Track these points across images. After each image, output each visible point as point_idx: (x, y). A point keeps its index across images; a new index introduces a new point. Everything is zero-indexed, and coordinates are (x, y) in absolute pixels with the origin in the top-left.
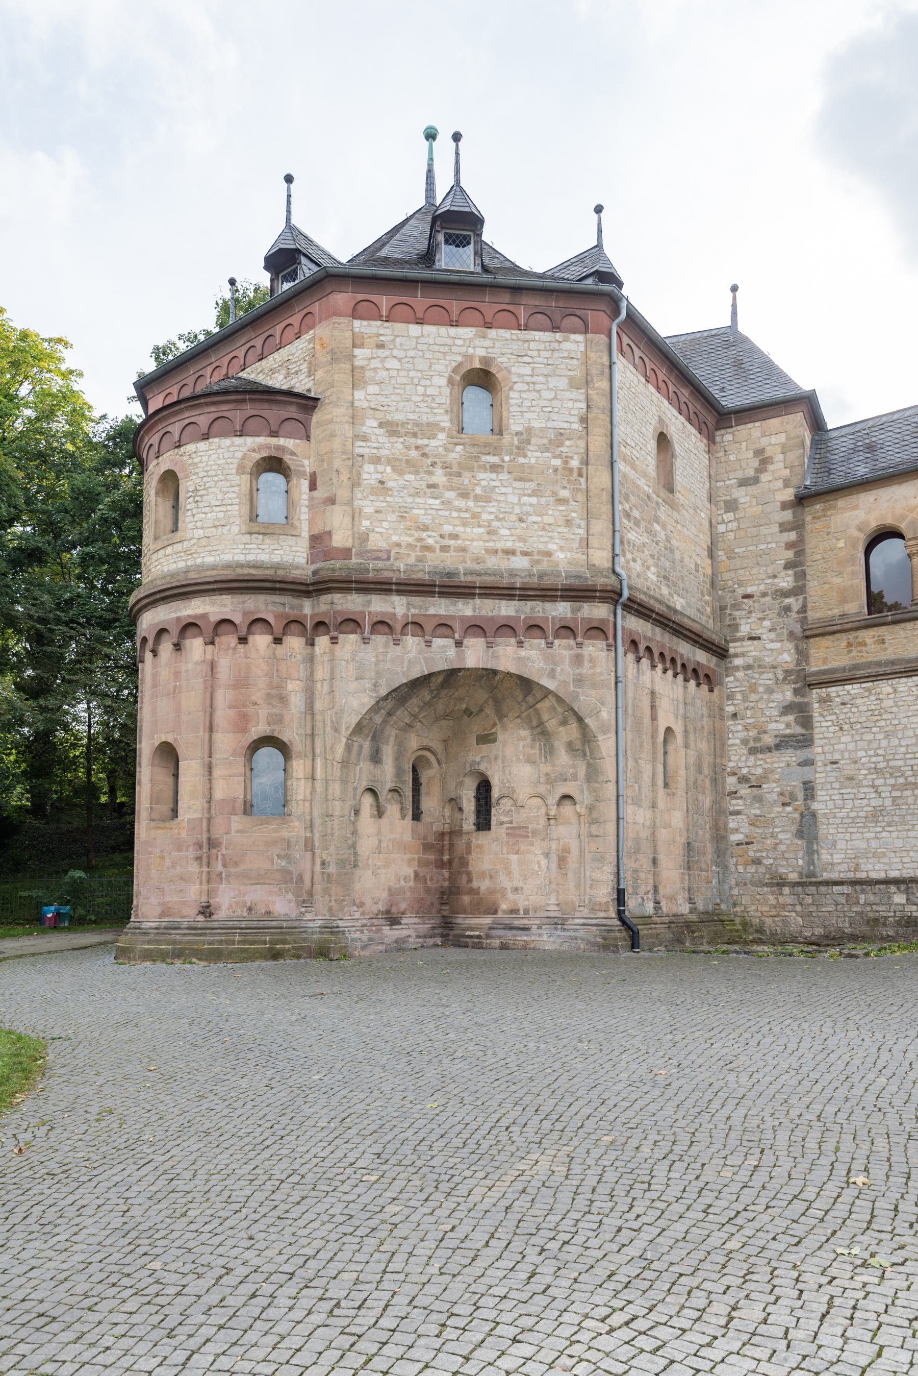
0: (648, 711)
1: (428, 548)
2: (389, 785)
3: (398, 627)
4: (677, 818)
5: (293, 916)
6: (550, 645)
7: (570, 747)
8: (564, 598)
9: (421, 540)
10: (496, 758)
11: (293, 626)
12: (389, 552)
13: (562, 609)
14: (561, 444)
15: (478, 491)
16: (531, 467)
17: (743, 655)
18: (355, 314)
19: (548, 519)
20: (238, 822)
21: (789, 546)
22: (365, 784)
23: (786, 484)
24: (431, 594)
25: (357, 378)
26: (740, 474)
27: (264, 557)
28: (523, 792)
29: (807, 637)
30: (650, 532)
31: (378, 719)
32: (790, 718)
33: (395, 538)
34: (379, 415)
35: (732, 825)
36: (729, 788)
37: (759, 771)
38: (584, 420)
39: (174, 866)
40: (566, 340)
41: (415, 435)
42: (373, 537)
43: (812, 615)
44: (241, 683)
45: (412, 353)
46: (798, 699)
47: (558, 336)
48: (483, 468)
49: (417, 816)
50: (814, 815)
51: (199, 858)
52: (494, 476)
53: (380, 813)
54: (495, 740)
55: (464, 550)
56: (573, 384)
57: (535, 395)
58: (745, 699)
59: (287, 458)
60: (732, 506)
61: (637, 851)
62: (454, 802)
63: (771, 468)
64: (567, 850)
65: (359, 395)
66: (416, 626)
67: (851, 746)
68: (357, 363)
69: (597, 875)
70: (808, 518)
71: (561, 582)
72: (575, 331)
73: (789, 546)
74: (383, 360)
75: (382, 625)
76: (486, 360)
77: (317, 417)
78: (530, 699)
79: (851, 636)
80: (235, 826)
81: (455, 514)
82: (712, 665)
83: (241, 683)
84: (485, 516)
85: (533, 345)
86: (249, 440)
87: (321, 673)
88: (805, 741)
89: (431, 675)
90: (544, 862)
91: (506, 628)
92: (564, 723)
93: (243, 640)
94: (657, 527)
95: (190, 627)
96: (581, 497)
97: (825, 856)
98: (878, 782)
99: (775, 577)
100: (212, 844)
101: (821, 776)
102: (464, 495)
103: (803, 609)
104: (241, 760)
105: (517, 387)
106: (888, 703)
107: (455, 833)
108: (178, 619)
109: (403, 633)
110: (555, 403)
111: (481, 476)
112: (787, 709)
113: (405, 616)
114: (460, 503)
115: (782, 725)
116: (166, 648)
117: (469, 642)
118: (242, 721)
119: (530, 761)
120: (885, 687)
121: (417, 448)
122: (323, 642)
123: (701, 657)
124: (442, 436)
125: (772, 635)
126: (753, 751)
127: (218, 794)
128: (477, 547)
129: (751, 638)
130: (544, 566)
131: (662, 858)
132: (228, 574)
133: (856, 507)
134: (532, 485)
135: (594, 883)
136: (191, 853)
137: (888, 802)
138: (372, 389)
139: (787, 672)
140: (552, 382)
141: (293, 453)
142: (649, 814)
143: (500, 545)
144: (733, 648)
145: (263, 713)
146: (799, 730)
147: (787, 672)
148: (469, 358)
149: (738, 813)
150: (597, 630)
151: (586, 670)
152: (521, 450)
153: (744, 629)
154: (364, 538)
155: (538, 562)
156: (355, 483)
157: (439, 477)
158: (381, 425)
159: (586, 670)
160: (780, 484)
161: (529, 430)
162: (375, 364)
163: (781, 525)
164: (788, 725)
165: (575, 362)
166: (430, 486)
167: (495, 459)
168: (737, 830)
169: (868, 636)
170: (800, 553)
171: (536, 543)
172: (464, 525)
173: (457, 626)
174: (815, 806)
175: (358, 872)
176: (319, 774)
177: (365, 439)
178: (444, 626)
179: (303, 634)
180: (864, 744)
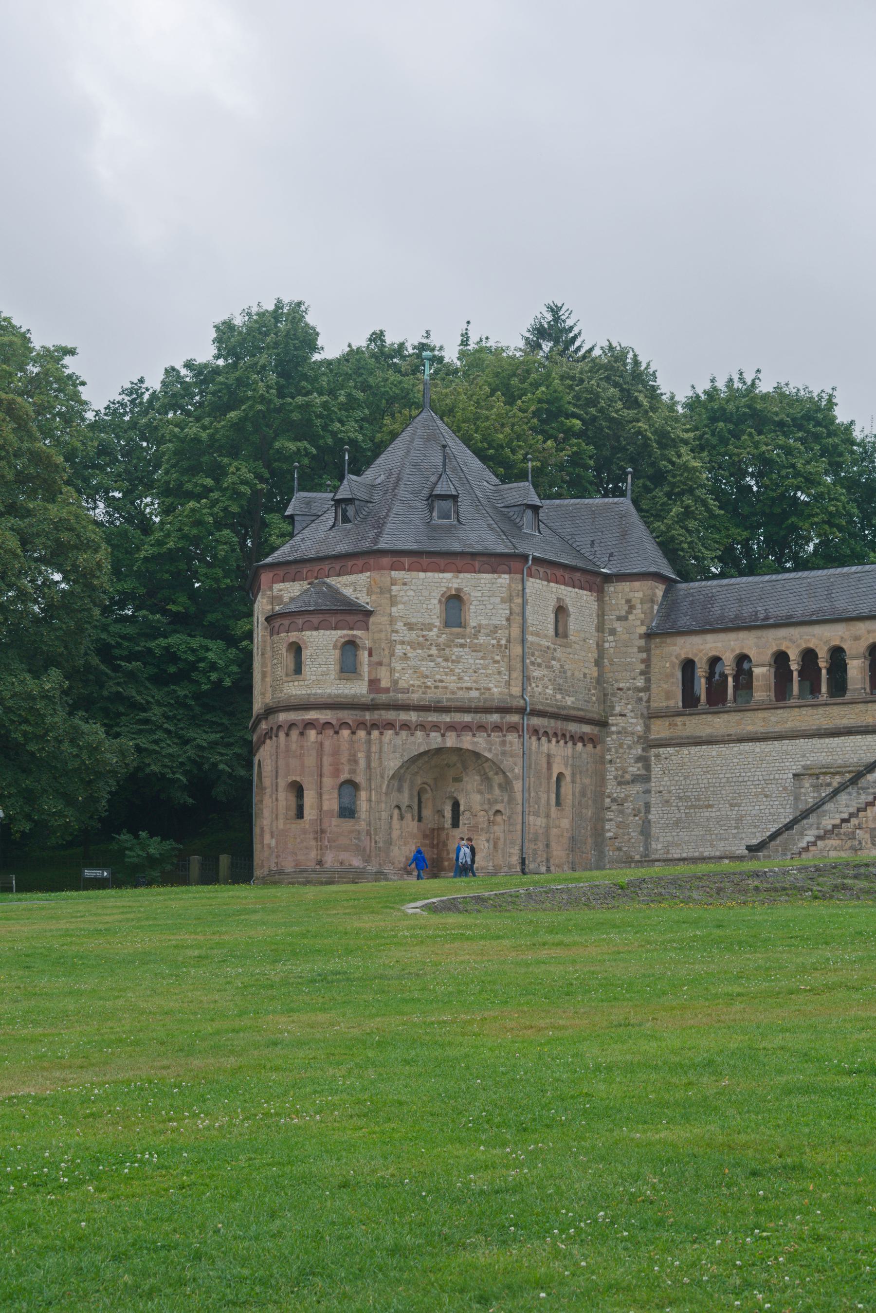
0: (545, 766)
1: (428, 687)
2: (406, 804)
3: (413, 727)
4: (565, 823)
5: (361, 867)
6: (489, 736)
7: (500, 785)
8: (496, 712)
9: (424, 683)
10: (462, 790)
11: (361, 726)
12: (408, 689)
13: (495, 718)
14: (497, 632)
15: (454, 657)
17: (616, 725)
18: (393, 568)
20: (335, 821)
21: (643, 661)
22: (395, 803)
23: (642, 624)
24: (429, 711)
25: (393, 601)
26: (617, 613)
27: (346, 691)
28: (477, 807)
29: (650, 718)
30: (549, 667)
31: (402, 771)
32: (640, 765)
33: (411, 682)
34: (404, 620)
35: (607, 827)
36: (606, 805)
37: (623, 795)
38: (508, 619)
39: (302, 842)
40: (500, 577)
41: (422, 630)
42: (400, 682)
43: (654, 705)
44: (336, 753)
45: (420, 587)
46: (644, 754)
47: (495, 576)
48: (456, 646)
49: (420, 819)
50: (649, 822)
51: (316, 839)
52: (461, 650)
53: (402, 818)
54: (462, 781)
55: (446, 688)
56: (503, 601)
58: (617, 752)
59: (358, 641)
60: (613, 632)
61: (536, 840)
62: (440, 813)
63: (634, 612)
64: (498, 839)
65: (394, 609)
66: (422, 726)
67: (668, 783)
68: (393, 593)
69: (512, 851)
70: (653, 646)
71: (495, 704)
72: (504, 573)
73: (643, 661)
75: (405, 726)
76: (459, 590)
77: (372, 619)
78: (479, 761)
79: (671, 719)
80: (334, 823)
81: (442, 670)
82: (595, 732)
83: (336, 753)
84: (457, 671)
85: (482, 581)
86: (340, 633)
87: (374, 748)
88: (646, 779)
89: (429, 751)
90: (486, 845)
92: (497, 774)
93: (337, 733)
94: (553, 662)
95: (310, 724)
96: (506, 660)
97: (654, 846)
98: (680, 804)
99: (634, 679)
100: (323, 831)
101: (654, 799)
102: (446, 660)
103: (648, 701)
104: (336, 791)
105: (474, 603)
106: (686, 760)
107: (441, 829)
108: (303, 720)
109: (416, 729)
110: (493, 611)
111: (455, 650)
112: (639, 759)
113: (417, 721)
114: (444, 664)
115: (635, 769)
116: (295, 734)
117: (448, 734)
118: (336, 772)
119: (480, 792)
120: (685, 751)
121: (423, 636)
122: (375, 733)
124: (435, 630)
125: (632, 714)
126: (620, 784)
127: (325, 807)
128: (452, 686)
129: (621, 715)
130: (487, 695)
131: (553, 844)
132: (330, 701)
133: (675, 645)
134: (481, 654)
135: (510, 855)
136: (312, 836)
137: (683, 815)
138: (401, 606)
139: (639, 737)
140: (492, 600)
141: (361, 638)
142: (544, 820)
143: (464, 685)
144: (612, 720)
145: (346, 768)
146: (643, 772)
147: (639, 737)
148: (449, 589)
149: (611, 820)
150: (513, 728)
151: (508, 748)
152: (476, 636)
153: (618, 709)
154: (396, 682)
155: (483, 693)
156: (392, 654)
157: (434, 651)
158: (405, 625)
159: (508, 748)
160: (639, 623)
161: (480, 626)
162: (402, 593)
163: (639, 648)
164: (639, 769)
165: (504, 589)
166: (429, 656)
167: (462, 641)
168: (609, 830)
169: (679, 720)
170: (648, 666)
171: (483, 684)
172: (446, 675)
173: (442, 726)
174: (650, 817)
175: (392, 847)
176: (373, 798)
177: (397, 632)
178: (436, 727)
179: (365, 729)
180: (673, 782)
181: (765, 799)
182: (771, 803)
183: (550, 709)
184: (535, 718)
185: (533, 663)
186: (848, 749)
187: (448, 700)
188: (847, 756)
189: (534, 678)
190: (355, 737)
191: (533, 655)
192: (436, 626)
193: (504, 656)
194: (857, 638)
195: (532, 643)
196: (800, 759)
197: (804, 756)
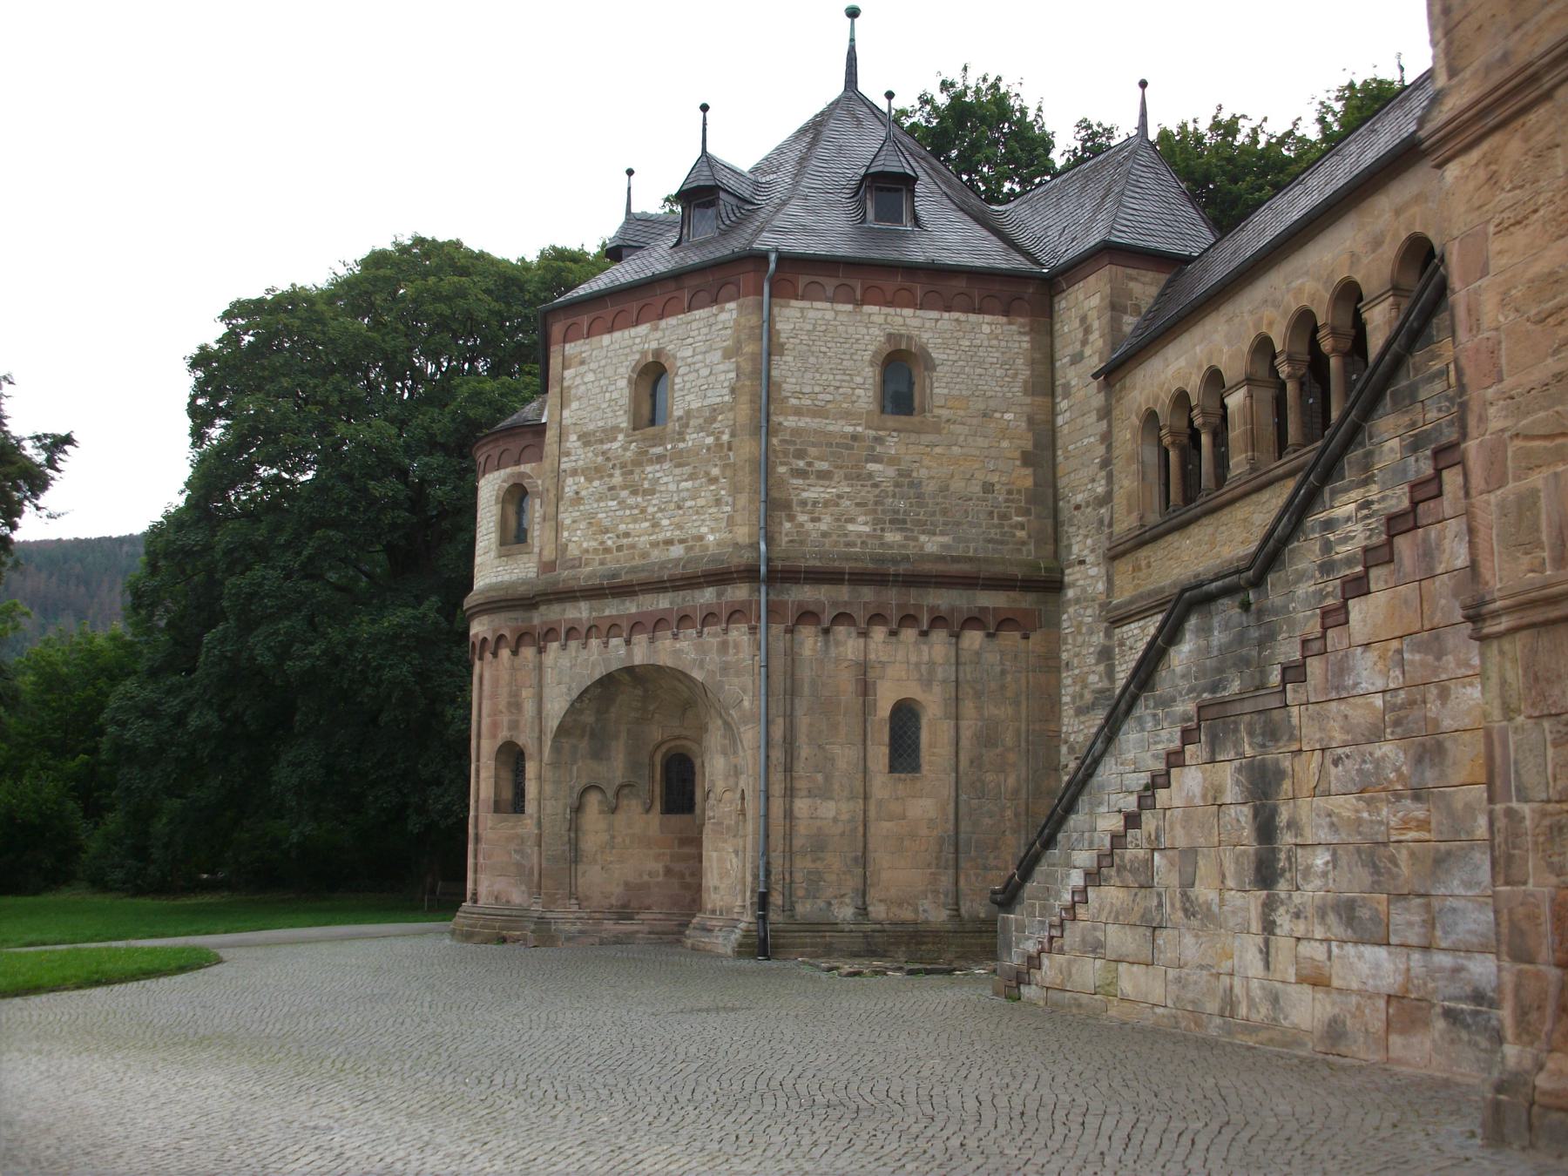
1: (607, 550)
6: (700, 634)
8: (710, 584)
13: (708, 595)
14: (714, 420)
15: (646, 485)
16: (688, 450)
19: (701, 502)
24: (604, 596)
33: (585, 545)
34: (578, 428)
38: (733, 391)
40: (722, 310)
42: (571, 546)
47: (715, 309)
48: (650, 462)
52: (658, 467)
55: (633, 546)
56: (727, 355)
57: (695, 374)
59: (526, 483)
74: (583, 375)
76: (658, 353)
81: (628, 512)
84: (651, 510)
91: (657, 624)
96: (729, 473)
102: (634, 493)
105: (681, 371)
110: (711, 379)
111: (649, 469)
113: (589, 619)
121: (603, 453)
122: (528, 652)
123: (1026, 601)
124: (621, 437)
130: (697, 552)
134: (687, 470)
140: (710, 358)
141: (530, 477)
143: (661, 537)
150: (736, 614)
151: (730, 658)
152: (681, 437)
154: (562, 548)
157: (617, 479)
165: (729, 331)
166: (611, 489)
167: (658, 450)
172: (635, 521)
178: (613, 628)
183: (847, 566)
184: (807, 588)
185: (801, 474)
187: (633, 570)
189: (804, 503)
190: (518, 661)
191: (800, 454)
192: (621, 430)
193: (725, 466)
195: (796, 432)
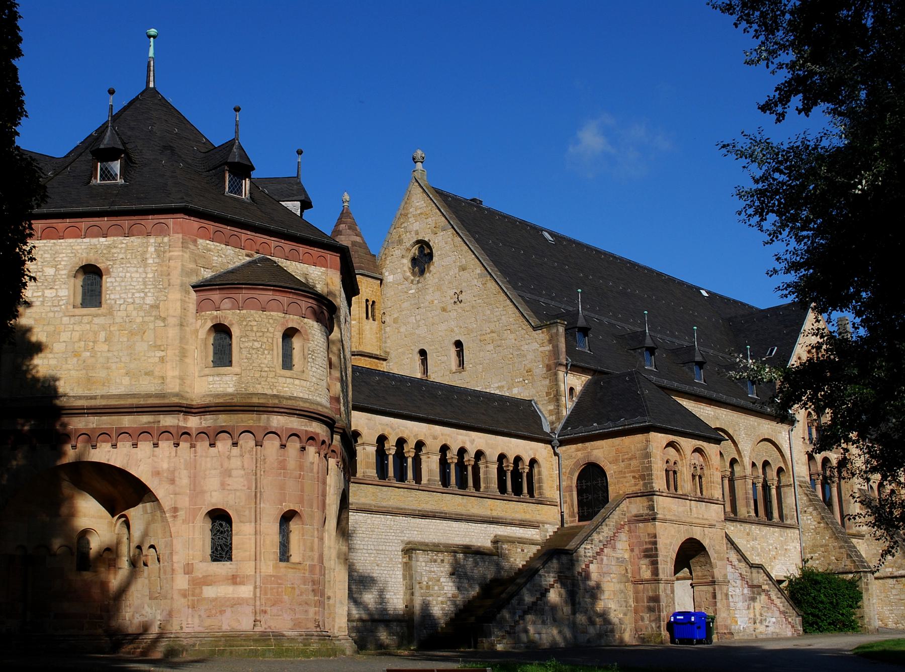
108: (306, 431)
181: (376, 568)
182: (381, 572)
186: (432, 530)
188: (431, 536)
194: (435, 438)
196: (400, 535)
197: (402, 532)
